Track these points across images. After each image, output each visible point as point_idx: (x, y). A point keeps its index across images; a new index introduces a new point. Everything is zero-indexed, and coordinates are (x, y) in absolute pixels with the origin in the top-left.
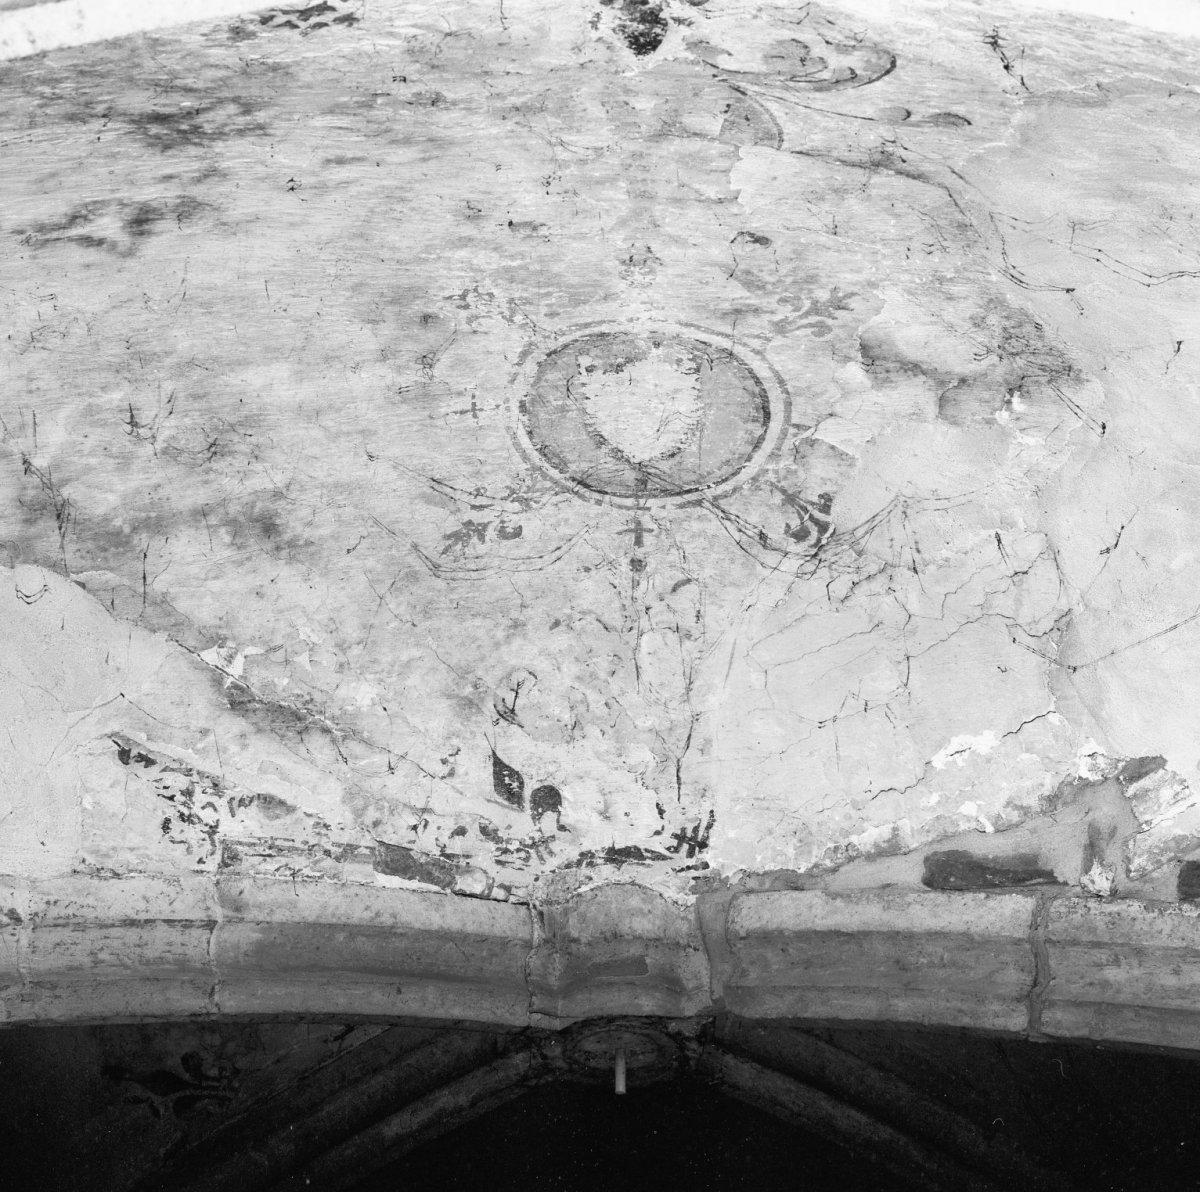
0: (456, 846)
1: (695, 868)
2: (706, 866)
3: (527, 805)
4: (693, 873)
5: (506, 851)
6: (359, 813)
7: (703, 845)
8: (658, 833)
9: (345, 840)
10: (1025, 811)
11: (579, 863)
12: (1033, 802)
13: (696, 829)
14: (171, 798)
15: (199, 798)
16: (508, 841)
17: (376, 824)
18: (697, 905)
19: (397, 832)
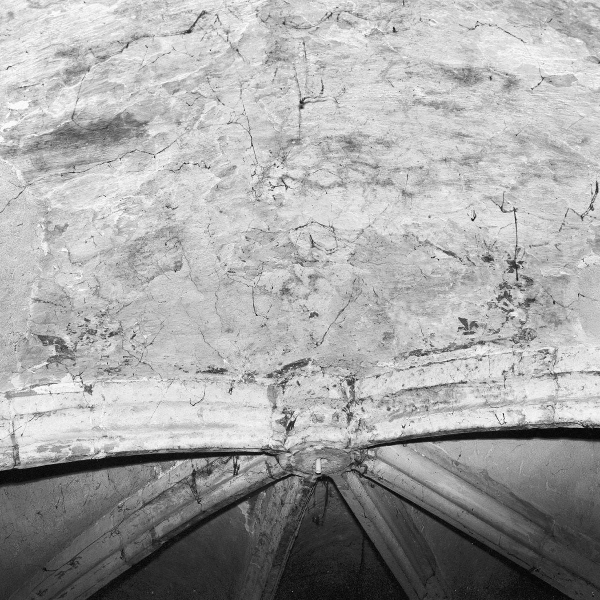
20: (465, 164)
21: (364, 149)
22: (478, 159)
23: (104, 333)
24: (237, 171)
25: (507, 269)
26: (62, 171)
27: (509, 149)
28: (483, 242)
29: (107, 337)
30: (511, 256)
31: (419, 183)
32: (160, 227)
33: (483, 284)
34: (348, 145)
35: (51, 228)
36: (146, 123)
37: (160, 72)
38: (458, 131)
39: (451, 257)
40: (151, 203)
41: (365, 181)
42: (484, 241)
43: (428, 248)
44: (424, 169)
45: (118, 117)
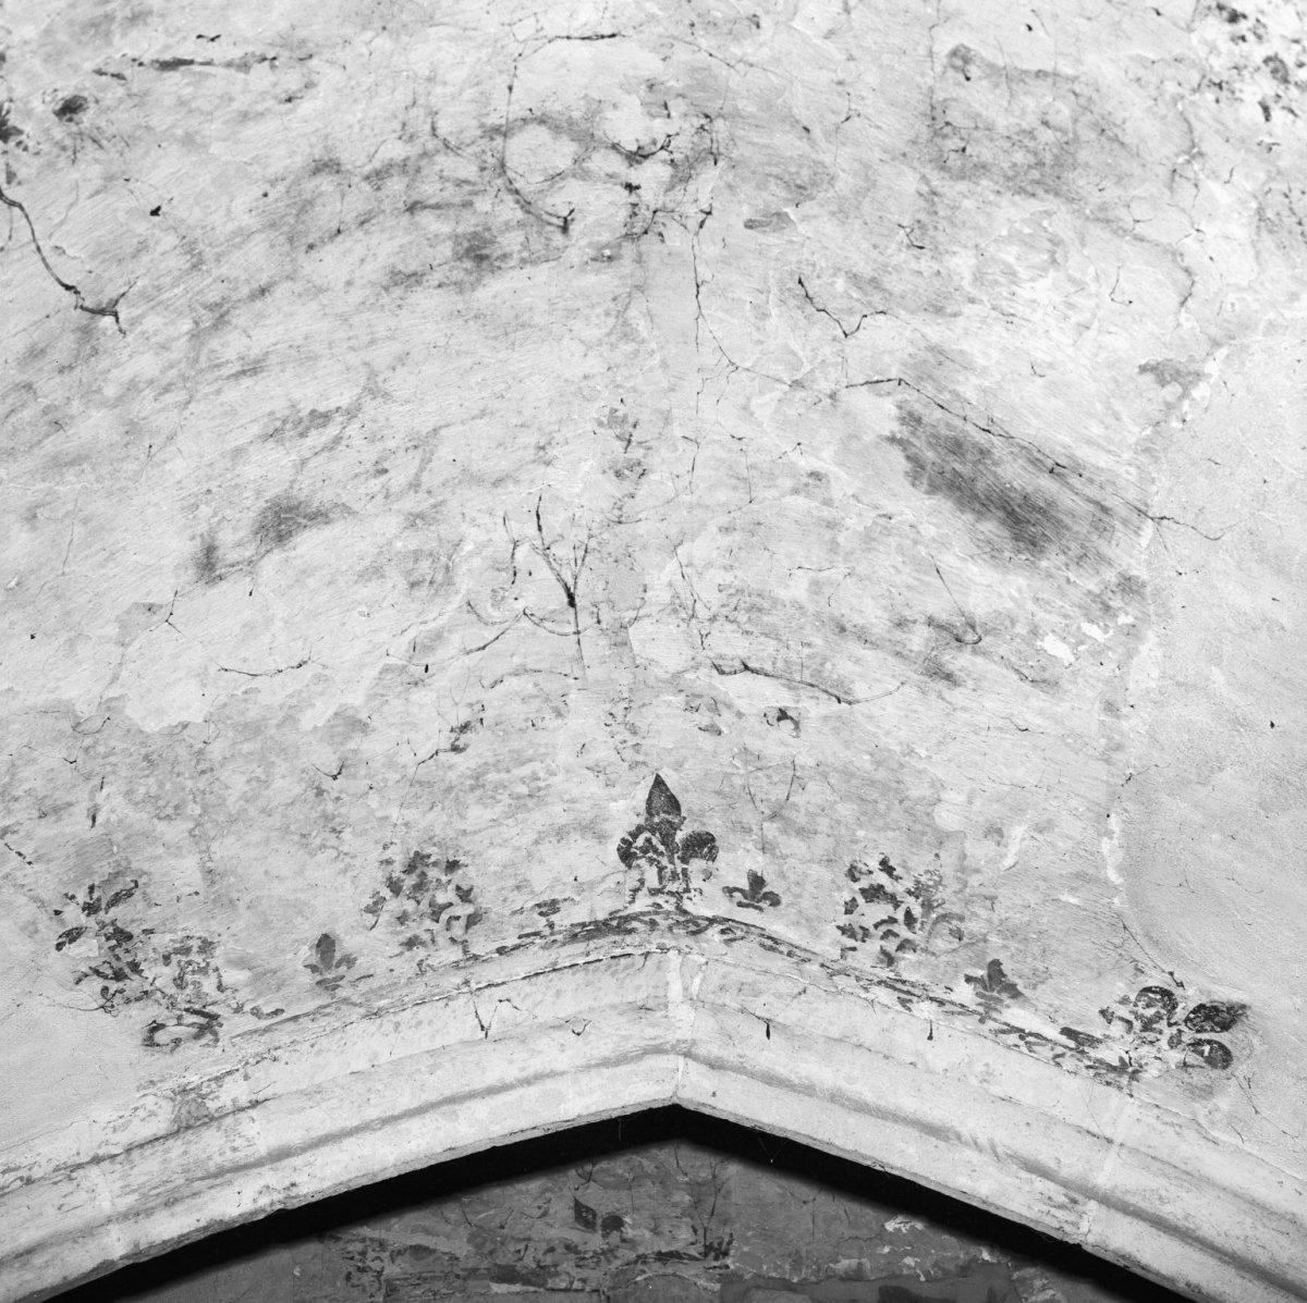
0: (548, 1260)
1: (720, 1268)
2: (727, 1267)
3: (599, 1228)
4: (718, 1271)
5: (584, 1258)
6: (479, 1247)
7: (726, 1254)
8: (692, 1244)
9: (470, 1266)
10: (946, 1272)
11: (636, 1262)
12: (951, 1267)
13: (720, 1244)
14: (352, 1258)
15: (371, 1254)
16: (585, 1252)
17: (491, 1253)
18: (722, 1294)
19: (506, 1258)
20: (218, 305)
21: (446, 250)
22: (196, 336)
23: (1250, 37)
24: (746, 212)
25: (8, 112)
26: (1074, 480)
27: (149, 393)
28: (104, 143)
29: (1250, 22)
30: (19, 151)
31: (306, 206)
32: (962, 186)
33: (48, 32)
34: (484, 252)
35: (1170, 392)
36: (892, 440)
37: (828, 535)
38: (260, 376)
39: (167, 57)
40: (956, 260)
41: (436, 158)
42: (101, 147)
43: (236, 54)
44: (304, 248)
45: (933, 489)
